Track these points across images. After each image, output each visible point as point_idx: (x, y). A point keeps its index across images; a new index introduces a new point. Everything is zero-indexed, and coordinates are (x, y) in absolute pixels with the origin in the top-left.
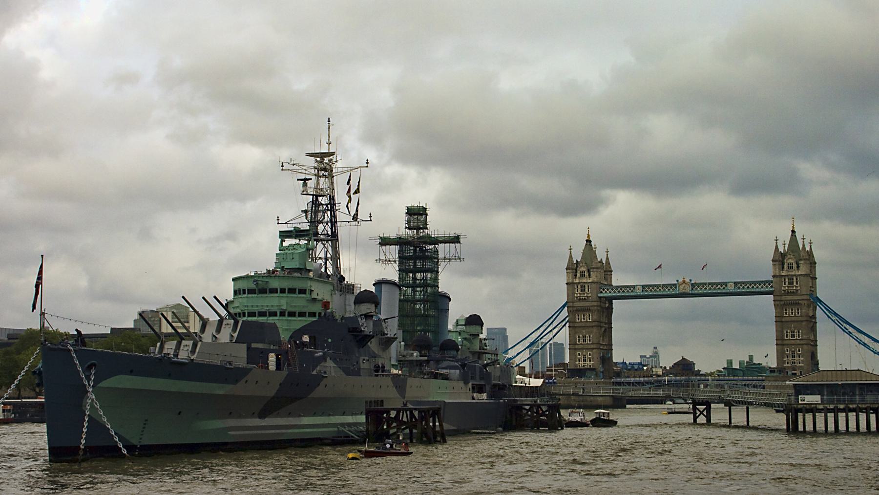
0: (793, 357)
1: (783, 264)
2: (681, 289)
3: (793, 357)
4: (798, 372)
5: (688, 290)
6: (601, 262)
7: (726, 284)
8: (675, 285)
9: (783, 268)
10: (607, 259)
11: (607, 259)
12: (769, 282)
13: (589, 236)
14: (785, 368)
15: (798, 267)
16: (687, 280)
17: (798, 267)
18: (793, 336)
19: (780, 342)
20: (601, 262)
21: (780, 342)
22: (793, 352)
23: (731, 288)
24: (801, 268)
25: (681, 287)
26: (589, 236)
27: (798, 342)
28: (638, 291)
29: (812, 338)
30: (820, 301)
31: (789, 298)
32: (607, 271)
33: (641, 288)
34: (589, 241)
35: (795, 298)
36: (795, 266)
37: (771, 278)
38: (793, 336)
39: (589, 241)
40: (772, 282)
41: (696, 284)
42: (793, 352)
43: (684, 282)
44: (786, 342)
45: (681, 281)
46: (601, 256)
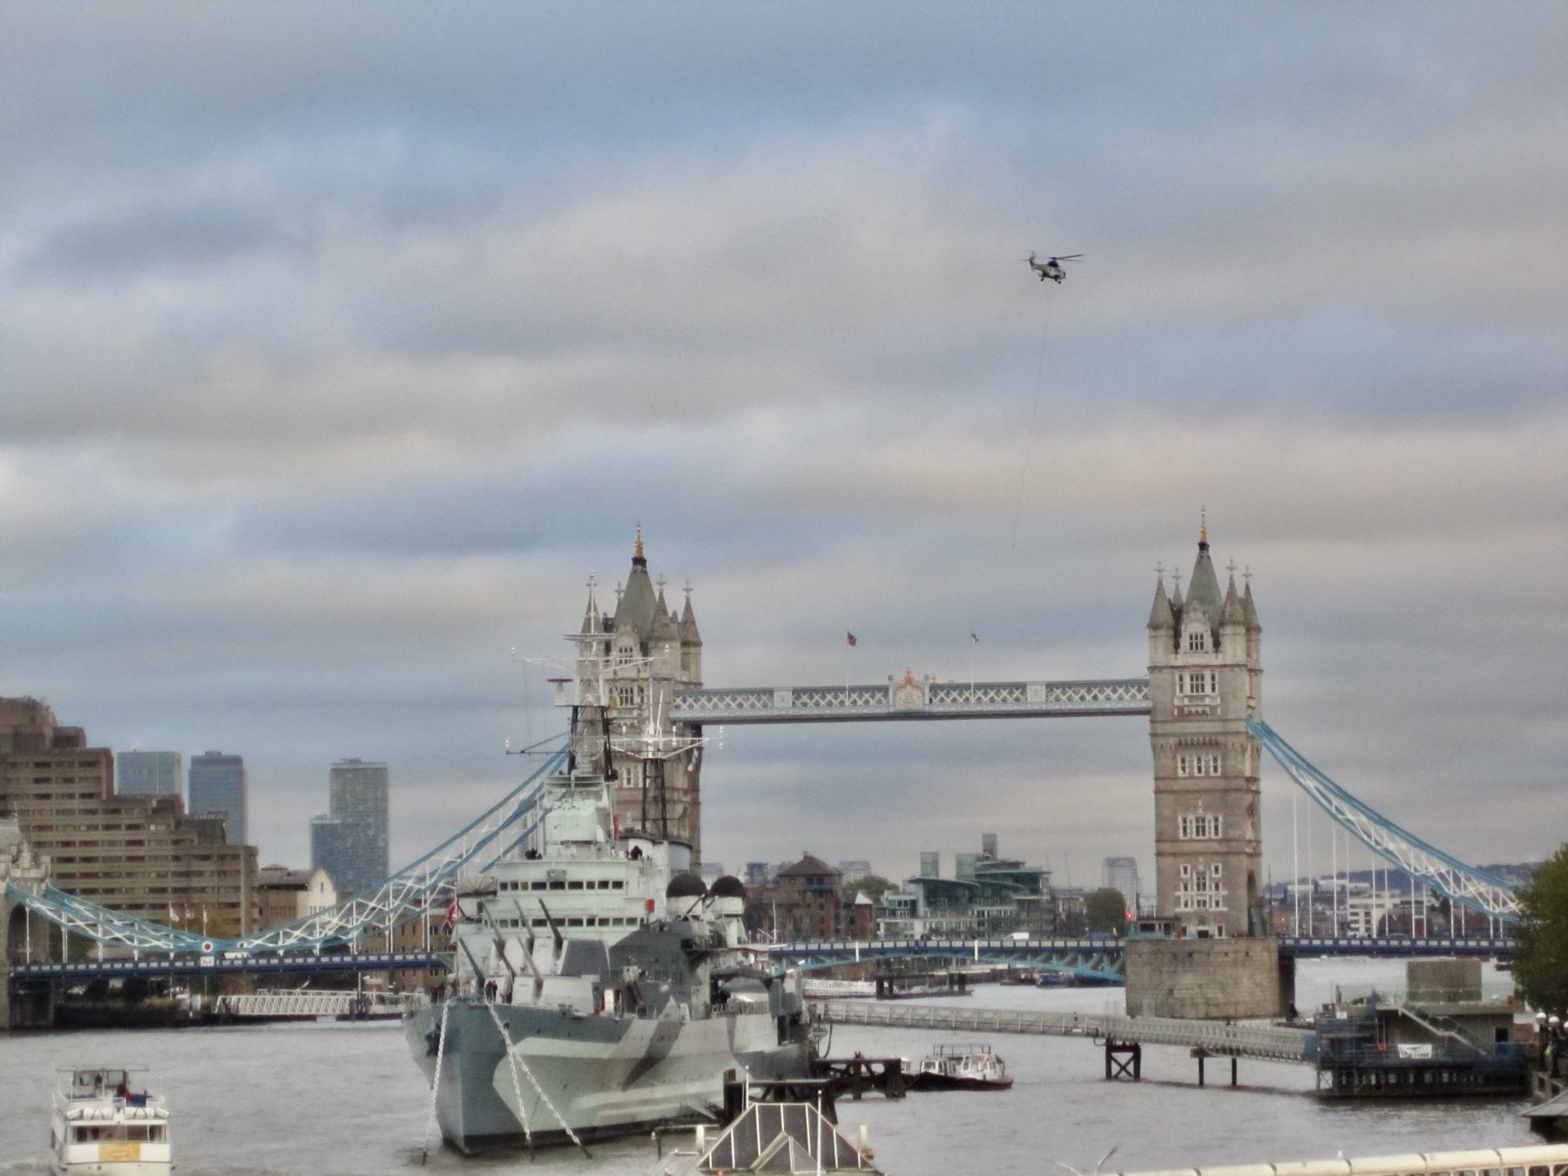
0: (1201, 886)
1: (1177, 635)
2: (899, 702)
3: (1201, 886)
4: (1212, 929)
5: (919, 702)
6: (674, 619)
7: (1022, 687)
8: (884, 690)
9: (1177, 646)
10: (688, 609)
11: (688, 609)
12: (1139, 684)
13: (640, 548)
14: (1177, 918)
15: (1217, 644)
16: (918, 677)
17: (1217, 644)
18: (1201, 830)
19: (1167, 847)
20: (674, 619)
21: (1167, 847)
22: (1201, 877)
23: (1036, 698)
24: (1227, 643)
25: (902, 695)
26: (640, 548)
27: (1215, 846)
28: (783, 704)
29: (1249, 835)
30: (1271, 734)
31: (1191, 727)
32: (690, 643)
33: (790, 697)
34: (639, 561)
35: (1210, 727)
36: (1208, 641)
37: (1141, 672)
38: (1201, 830)
39: (639, 561)
40: (1146, 684)
41: (942, 687)
42: (1201, 877)
43: (909, 681)
44: (1186, 847)
45: (900, 678)
46: (675, 605)
